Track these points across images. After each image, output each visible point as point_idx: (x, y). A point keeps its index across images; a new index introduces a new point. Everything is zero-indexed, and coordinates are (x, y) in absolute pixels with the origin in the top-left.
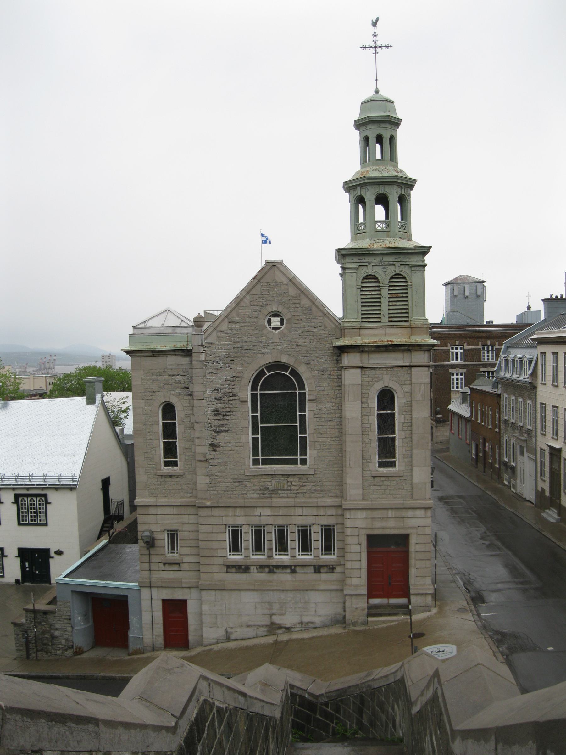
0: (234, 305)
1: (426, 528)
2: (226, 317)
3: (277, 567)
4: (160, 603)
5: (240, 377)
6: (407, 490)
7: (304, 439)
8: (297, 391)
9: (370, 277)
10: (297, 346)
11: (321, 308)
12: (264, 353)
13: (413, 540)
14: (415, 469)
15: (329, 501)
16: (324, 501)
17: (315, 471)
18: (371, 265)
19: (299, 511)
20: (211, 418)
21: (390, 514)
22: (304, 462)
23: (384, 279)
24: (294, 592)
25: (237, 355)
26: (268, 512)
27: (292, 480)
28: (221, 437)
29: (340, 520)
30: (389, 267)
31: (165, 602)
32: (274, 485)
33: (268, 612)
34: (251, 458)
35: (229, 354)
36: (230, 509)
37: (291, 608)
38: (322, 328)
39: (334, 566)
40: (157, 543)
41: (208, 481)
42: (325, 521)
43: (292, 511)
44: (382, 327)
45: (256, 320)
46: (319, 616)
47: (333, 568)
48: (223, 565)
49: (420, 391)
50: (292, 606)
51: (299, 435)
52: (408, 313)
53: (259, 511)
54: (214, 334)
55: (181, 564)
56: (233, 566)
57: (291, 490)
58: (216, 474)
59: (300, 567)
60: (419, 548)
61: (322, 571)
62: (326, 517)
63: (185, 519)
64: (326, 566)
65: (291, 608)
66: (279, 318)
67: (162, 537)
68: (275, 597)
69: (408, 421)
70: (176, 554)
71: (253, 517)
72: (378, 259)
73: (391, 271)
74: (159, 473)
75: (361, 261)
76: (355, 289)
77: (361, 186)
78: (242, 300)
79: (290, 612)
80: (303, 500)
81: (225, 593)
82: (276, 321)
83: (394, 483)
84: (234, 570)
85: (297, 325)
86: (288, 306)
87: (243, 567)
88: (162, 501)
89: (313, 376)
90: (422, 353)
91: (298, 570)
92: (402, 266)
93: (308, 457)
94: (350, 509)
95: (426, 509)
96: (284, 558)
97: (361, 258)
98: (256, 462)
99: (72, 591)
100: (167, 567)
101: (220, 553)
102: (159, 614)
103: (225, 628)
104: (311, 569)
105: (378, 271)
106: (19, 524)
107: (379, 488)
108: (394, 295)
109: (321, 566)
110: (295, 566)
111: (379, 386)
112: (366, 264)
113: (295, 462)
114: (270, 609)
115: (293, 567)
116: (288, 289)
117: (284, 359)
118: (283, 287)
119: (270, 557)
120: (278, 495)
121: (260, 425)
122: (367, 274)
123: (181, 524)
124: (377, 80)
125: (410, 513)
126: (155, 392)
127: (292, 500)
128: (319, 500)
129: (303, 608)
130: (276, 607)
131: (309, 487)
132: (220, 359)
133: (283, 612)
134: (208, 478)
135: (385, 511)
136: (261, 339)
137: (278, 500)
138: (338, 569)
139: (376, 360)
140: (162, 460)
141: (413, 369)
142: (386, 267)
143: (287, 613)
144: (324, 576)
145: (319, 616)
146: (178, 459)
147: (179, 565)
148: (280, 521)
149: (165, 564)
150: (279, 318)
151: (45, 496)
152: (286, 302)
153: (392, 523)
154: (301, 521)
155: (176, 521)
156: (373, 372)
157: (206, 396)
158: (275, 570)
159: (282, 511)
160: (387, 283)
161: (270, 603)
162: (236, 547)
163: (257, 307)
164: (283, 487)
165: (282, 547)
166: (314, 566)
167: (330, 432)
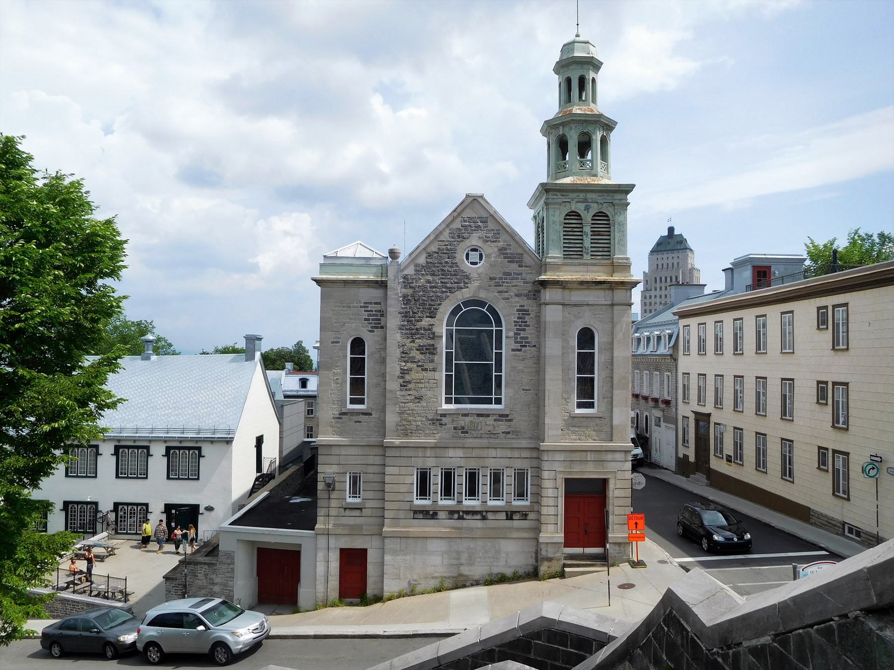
0: (432, 238)
1: (626, 472)
2: (424, 249)
3: (467, 513)
4: (338, 552)
6: (606, 432)
7: (499, 378)
8: (494, 328)
9: (572, 214)
11: (522, 244)
13: (611, 485)
15: (524, 443)
16: (519, 443)
17: (511, 411)
18: (574, 202)
19: (492, 453)
21: (590, 456)
22: (498, 401)
23: (587, 217)
24: (485, 539)
26: (460, 453)
29: (535, 463)
30: (592, 205)
31: (343, 552)
32: (468, 424)
33: (455, 562)
34: (444, 396)
36: (420, 449)
37: (480, 558)
39: (527, 513)
42: (519, 464)
43: (484, 453)
44: (584, 264)
46: (510, 567)
47: (526, 515)
48: (410, 510)
49: (621, 331)
50: (481, 556)
51: (494, 374)
52: (609, 251)
53: (451, 453)
55: (363, 510)
56: (421, 512)
58: (407, 412)
59: (491, 513)
60: (617, 493)
61: (514, 517)
62: (520, 459)
63: (371, 460)
64: (519, 512)
65: (480, 558)
66: (478, 253)
67: (343, 479)
68: (464, 545)
69: (609, 361)
70: (358, 499)
71: (443, 458)
72: (582, 195)
73: (594, 209)
74: (344, 410)
75: (563, 197)
76: (558, 224)
77: (563, 124)
78: (441, 233)
79: (479, 562)
81: (410, 541)
82: (474, 256)
84: (421, 516)
87: (431, 513)
90: (625, 291)
91: (490, 516)
93: (503, 397)
94: (548, 451)
97: (564, 194)
99: (238, 540)
100: (348, 513)
102: (335, 565)
103: (408, 580)
105: (580, 208)
106: (168, 478)
108: (596, 233)
109: (513, 513)
110: (487, 512)
111: (579, 325)
112: (569, 200)
113: (489, 401)
114: (458, 559)
115: (484, 514)
117: (482, 295)
119: (460, 502)
121: (454, 362)
122: (570, 211)
123: (366, 466)
124: (578, 25)
125: (609, 456)
127: (485, 441)
129: (494, 558)
130: (464, 557)
133: (472, 562)
135: (584, 454)
138: (531, 516)
139: (577, 296)
140: (348, 397)
141: (615, 307)
142: (589, 204)
143: (476, 563)
144: (516, 523)
145: (510, 567)
146: (365, 397)
147: (361, 511)
148: (473, 464)
149: (345, 509)
150: (478, 253)
151: (199, 449)
154: (493, 464)
155: (360, 462)
158: (465, 516)
159: (476, 453)
161: (459, 553)
162: (423, 491)
164: (477, 427)
165: (472, 492)
166: (506, 512)
167: (527, 371)
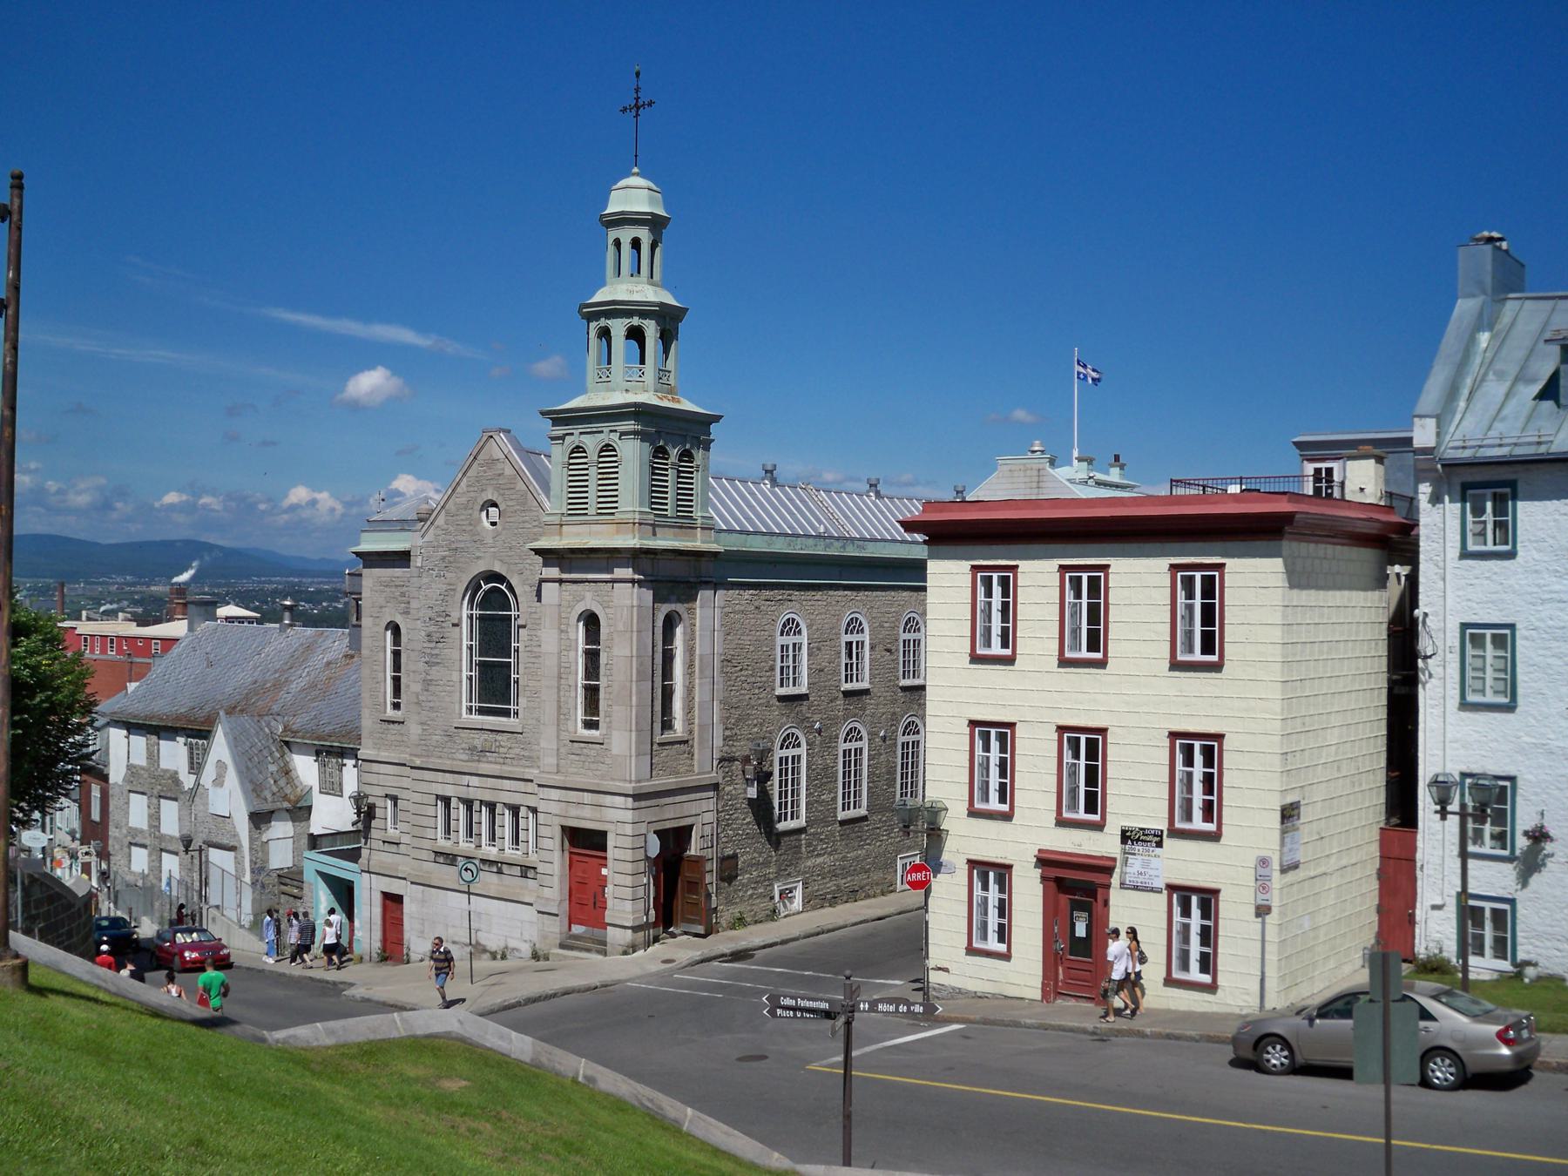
5: (454, 590)
10: (510, 548)
12: (478, 558)
14: (615, 734)
19: (507, 784)
20: (425, 645)
21: (587, 797)
23: (593, 454)
25: (451, 559)
27: (500, 738)
28: (435, 673)
35: (443, 558)
38: (536, 523)
40: (379, 812)
41: (420, 732)
45: (470, 511)
54: (431, 530)
57: (498, 753)
60: (619, 854)
63: (406, 783)
80: (510, 769)
83: (593, 753)
85: (512, 519)
86: (502, 492)
88: (383, 756)
89: (525, 592)
91: (505, 869)
92: (582, 436)
95: (626, 795)
96: (491, 852)
98: (470, 709)
101: (430, 833)
104: (517, 871)
107: (577, 758)
108: (605, 476)
110: (502, 863)
111: (580, 608)
116: (503, 469)
117: (498, 568)
118: (500, 466)
120: (485, 759)
125: (608, 799)
126: (381, 607)
127: (498, 767)
128: (527, 770)
131: (517, 751)
132: (436, 565)
134: (420, 727)
136: (476, 538)
137: (486, 765)
149: (384, 842)
152: (502, 486)
153: (587, 812)
156: (575, 587)
157: (421, 614)
160: (596, 458)
163: (472, 494)
